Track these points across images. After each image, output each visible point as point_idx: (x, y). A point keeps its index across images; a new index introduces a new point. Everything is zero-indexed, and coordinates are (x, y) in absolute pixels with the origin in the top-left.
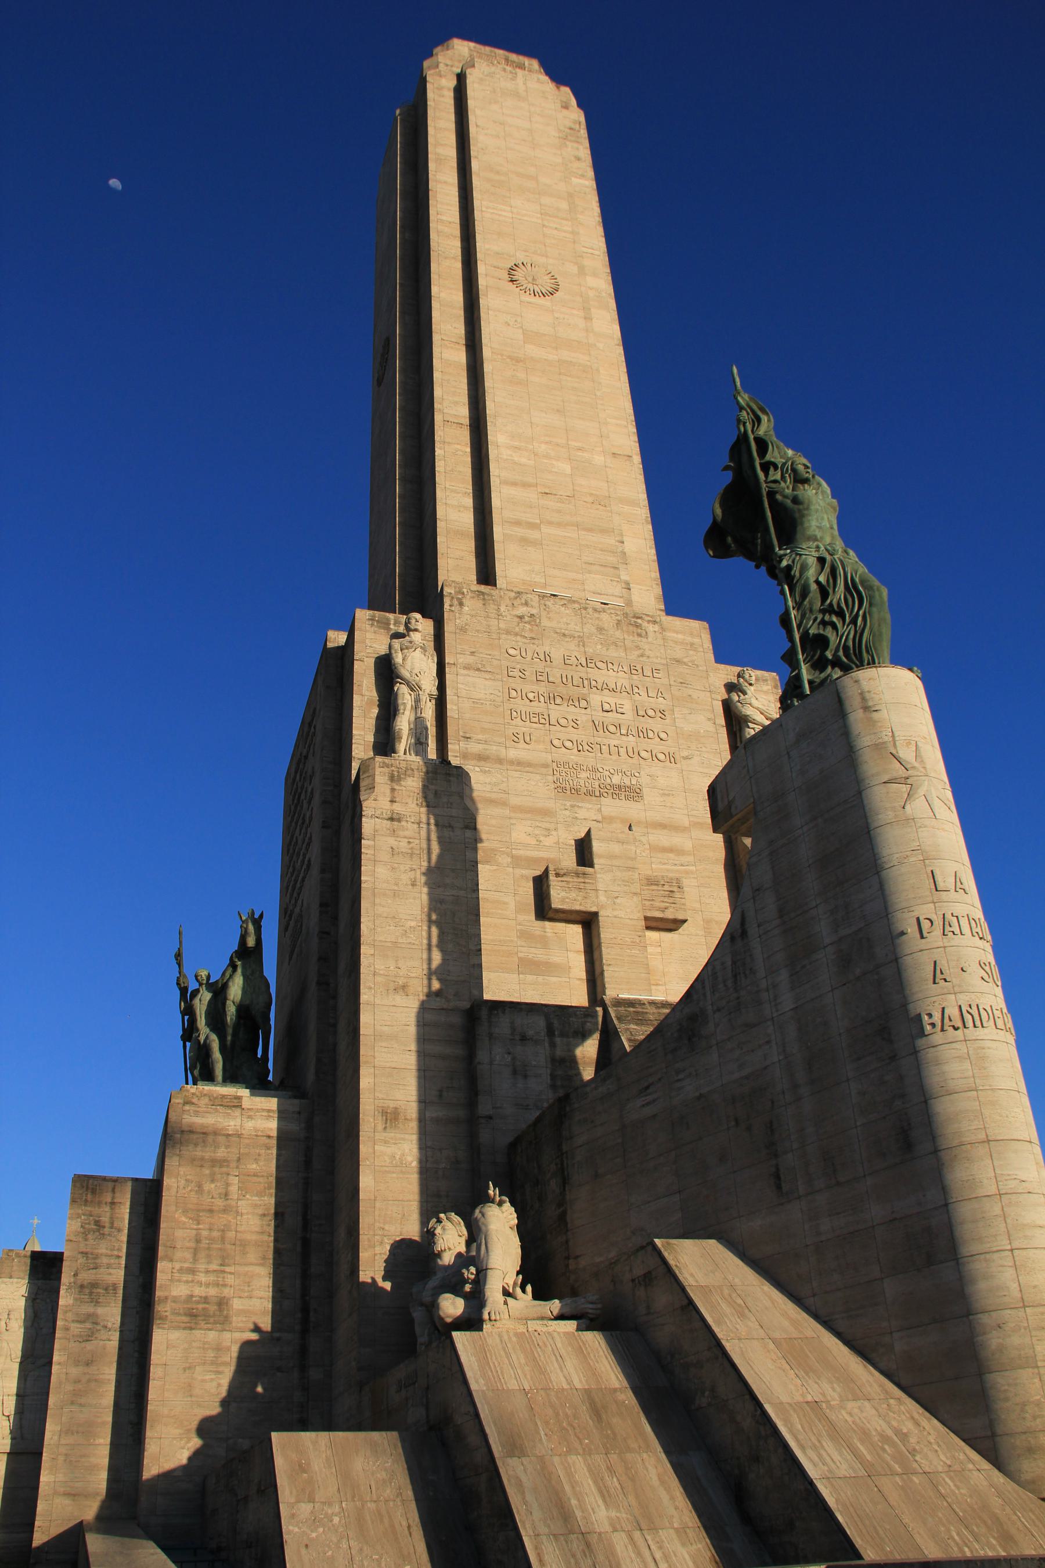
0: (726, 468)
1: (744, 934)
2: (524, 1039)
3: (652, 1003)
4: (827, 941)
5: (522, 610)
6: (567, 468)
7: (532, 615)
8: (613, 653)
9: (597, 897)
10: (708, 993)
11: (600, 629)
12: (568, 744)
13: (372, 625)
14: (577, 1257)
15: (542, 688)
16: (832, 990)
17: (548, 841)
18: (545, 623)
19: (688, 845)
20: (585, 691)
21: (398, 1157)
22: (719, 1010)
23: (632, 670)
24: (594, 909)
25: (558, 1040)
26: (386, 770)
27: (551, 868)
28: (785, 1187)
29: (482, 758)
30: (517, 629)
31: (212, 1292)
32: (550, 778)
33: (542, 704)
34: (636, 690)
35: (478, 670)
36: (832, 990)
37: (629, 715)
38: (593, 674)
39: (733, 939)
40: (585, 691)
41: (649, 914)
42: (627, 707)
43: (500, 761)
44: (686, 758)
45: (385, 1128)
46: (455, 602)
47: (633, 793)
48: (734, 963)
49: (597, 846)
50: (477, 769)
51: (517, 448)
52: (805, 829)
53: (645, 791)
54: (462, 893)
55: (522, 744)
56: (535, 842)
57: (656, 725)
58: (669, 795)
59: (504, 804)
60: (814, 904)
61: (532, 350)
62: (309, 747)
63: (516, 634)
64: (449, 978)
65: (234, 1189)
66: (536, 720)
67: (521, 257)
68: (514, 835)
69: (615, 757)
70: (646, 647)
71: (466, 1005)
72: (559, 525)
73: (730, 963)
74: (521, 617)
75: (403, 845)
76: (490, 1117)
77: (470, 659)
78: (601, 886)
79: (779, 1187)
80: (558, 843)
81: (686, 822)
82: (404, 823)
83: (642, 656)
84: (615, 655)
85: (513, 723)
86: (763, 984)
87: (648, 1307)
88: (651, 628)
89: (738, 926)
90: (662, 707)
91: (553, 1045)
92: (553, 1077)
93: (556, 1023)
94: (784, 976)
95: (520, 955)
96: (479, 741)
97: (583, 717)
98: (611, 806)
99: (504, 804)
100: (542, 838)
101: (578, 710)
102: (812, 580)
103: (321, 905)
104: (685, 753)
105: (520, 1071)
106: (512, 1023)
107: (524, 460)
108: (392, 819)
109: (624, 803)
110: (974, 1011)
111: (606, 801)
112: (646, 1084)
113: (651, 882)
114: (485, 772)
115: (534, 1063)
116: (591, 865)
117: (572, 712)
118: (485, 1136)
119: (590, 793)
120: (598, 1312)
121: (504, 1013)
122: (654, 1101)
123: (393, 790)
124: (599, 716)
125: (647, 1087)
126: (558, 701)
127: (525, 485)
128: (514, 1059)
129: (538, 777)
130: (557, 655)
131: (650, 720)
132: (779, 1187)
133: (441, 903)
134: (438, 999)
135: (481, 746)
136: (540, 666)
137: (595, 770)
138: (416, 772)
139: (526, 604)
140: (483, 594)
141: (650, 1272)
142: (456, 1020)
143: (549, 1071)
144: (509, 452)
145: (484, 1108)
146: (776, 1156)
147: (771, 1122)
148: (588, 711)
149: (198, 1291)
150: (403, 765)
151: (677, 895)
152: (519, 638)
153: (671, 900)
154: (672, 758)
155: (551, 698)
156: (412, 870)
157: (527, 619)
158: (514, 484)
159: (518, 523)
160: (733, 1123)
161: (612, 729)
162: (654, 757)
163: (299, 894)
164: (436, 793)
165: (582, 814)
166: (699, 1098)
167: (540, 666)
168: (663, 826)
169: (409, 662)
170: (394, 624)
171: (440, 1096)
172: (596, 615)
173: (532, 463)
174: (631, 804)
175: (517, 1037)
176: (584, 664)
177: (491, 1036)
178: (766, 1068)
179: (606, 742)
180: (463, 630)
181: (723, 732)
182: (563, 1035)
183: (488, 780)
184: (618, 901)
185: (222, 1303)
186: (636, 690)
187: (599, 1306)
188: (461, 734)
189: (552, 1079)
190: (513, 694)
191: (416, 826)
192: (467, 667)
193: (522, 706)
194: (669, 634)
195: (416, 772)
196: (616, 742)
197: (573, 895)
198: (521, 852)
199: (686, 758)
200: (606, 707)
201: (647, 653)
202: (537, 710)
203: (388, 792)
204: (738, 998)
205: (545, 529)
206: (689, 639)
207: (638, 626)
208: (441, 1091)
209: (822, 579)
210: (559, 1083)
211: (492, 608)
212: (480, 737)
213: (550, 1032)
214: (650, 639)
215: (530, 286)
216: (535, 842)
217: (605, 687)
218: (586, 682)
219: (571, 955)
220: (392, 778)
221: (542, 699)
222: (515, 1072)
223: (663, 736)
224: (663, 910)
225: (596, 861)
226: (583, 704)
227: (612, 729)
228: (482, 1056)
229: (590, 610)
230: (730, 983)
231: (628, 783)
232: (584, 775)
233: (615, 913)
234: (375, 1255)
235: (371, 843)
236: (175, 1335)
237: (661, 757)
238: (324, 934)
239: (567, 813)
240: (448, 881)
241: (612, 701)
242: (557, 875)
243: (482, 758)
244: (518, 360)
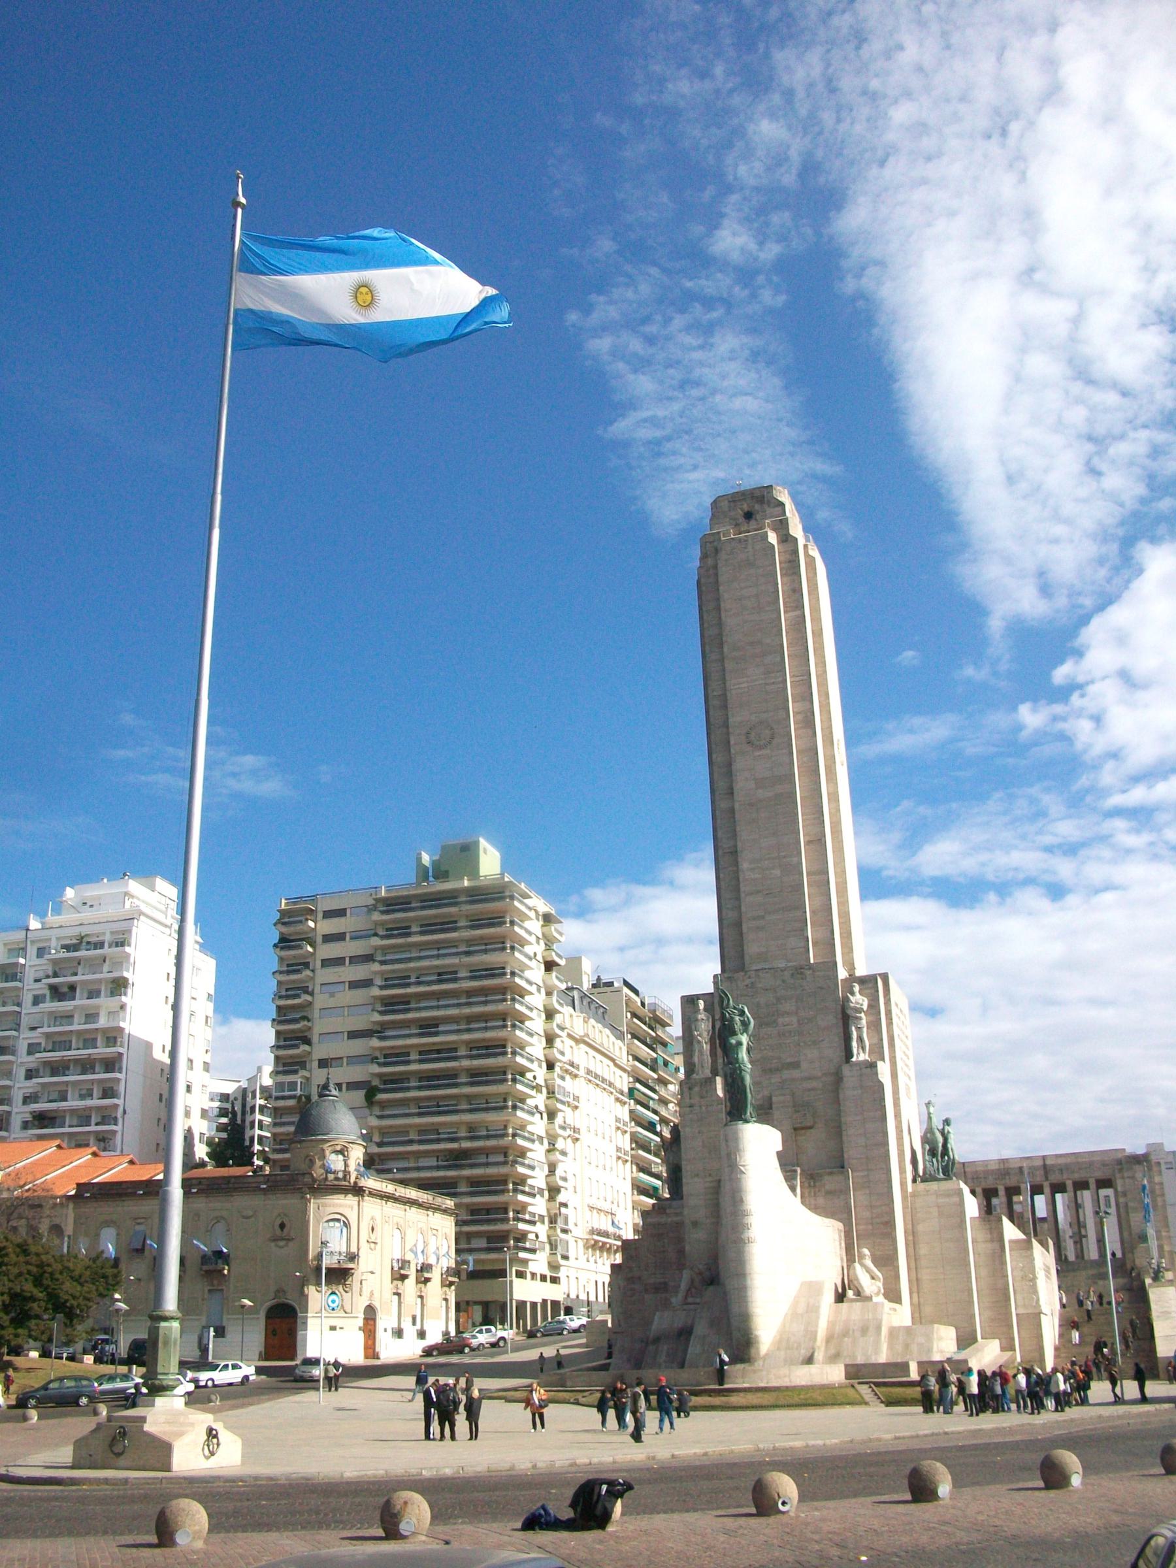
6: (777, 872)
47: (796, 1065)
61: (761, 794)
88: (808, 972)
98: (786, 1074)
107: (757, 876)
127: (758, 892)
154: (815, 1043)
158: (751, 894)
168: (810, 1078)
185: (665, 1284)
244: (751, 805)
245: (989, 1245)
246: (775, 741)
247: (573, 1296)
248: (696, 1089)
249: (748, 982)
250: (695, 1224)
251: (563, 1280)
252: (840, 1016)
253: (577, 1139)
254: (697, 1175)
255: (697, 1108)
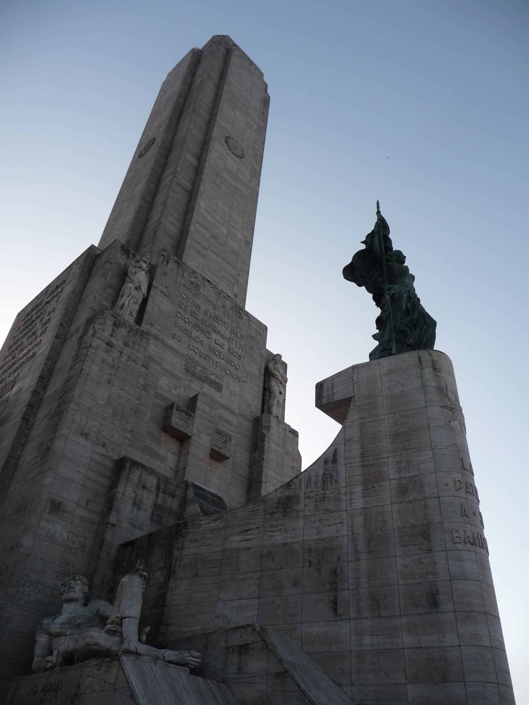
0: (363, 242)
1: (334, 461)
2: (144, 487)
3: (210, 492)
4: (392, 477)
5: (193, 280)
6: (225, 232)
7: (197, 285)
8: (226, 319)
9: (193, 429)
10: (303, 487)
11: (224, 306)
12: (196, 350)
13: (122, 250)
14: (168, 625)
15: (192, 319)
16: (392, 504)
17: (174, 392)
18: (202, 291)
19: (236, 423)
20: (210, 330)
21: (52, 532)
22: (309, 498)
23: (232, 331)
24: (189, 434)
25: (161, 494)
26: (113, 319)
27: (175, 405)
28: (340, 611)
29: (156, 337)
30: (189, 287)
32: (184, 362)
33: (190, 327)
34: (231, 341)
35: (166, 296)
36: (392, 504)
37: (225, 351)
38: (215, 324)
39: (326, 462)
40: (210, 330)
41: (213, 448)
42: (226, 346)
43: (163, 343)
44: (244, 382)
45: (50, 512)
46: (165, 260)
47: (219, 388)
48: (324, 474)
49: (199, 404)
50: (152, 342)
51: (207, 211)
52: (386, 417)
53: (224, 388)
54: (131, 398)
55: (176, 341)
56: (168, 390)
57: (236, 361)
58: (233, 395)
59: (159, 364)
60: (386, 456)
61: (226, 175)
62: (54, 296)
63: (188, 289)
64: (112, 439)
66: (185, 332)
67: (232, 135)
68: (159, 381)
69: (214, 367)
70: (241, 324)
71: (116, 457)
72: (215, 254)
73: (321, 474)
74: (192, 283)
75: (110, 360)
76: (114, 525)
77: (165, 290)
78: (196, 424)
79: (335, 610)
80: (178, 395)
81: (237, 411)
82: (114, 349)
83: (238, 327)
84: (227, 321)
85: (175, 328)
86: (344, 490)
87: (240, 669)
89: (331, 456)
90: (240, 354)
91: (157, 496)
92: (153, 514)
93: (162, 485)
94: (359, 489)
95: (146, 443)
96: (157, 329)
97: (206, 342)
98: (207, 389)
99: (159, 364)
100: (172, 389)
101: (205, 337)
102: (404, 305)
103: (40, 376)
104: (245, 380)
105: (137, 504)
106: (140, 476)
107: (208, 218)
108: (108, 344)
109: (212, 389)
110: (479, 537)
111: (205, 385)
112: (247, 528)
113: (219, 432)
114: (155, 345)
115: (145, 502)
116: (194, 412)
117: (202, 337)
118: (108, 536)
119: (199, 378)
120: (198, 664)
121: (138, 469)
122: (250, 539)
123: (113, 330)
124: (213, 344)
125: (248, 530)
126: (197, 328)
127: (206, 229)
128: (136, 496)
129: (178, 359)
130: (203, 307)
131: (234, 357)
132: (335, 610)
133: (119, 398)
134: (103, 449)
135: (157, 332)
136: (194, 309)
137: (204, 368)
138: (127, 327)
139: (196, 278)
140: (179, 263)
141: (247, 645)
142: (109, 464)
143: (151, 510)
144: (204, 211)
145: (113, 518)
146: (336, 590)
147: (336, 569)
148: (209, 340)
150: (122, 321)
151: (228, 444)
152: (188, 291)
153: (225, 445)
154: (239, 380)
155: (195, 326)
156: (110, 374)
157: (194, 285)
158: (202, 226)
159: (198, 243)
160: (307, 565)
161: (217, 353)
162: (231, 375)
163: (15, 371)
164: (134, 342)
165: (193, 386)
166: (284, 545)
167: (194, 309)
169: (138, 275)
170: (132, 255)
171: (87, 504)
172: (224, 299)
173: (212, 221)
174: (215, 392)
175: (141, 485)
176: (213, 317)
177: (128, 478)
178: (337, 537)
179: (213, 358)
180: (165, 274)
181: (262, 378)
182: (164, 492)
183: (155, 350)
184: (202, 435)
186: (231, 341)
187: (200, 660)
188: (150, 321)
189: (152, 515)
190: (179, 315)
191: (119, 353)
192: (162, 292)
193: (180, 322)
194: (251, 323)
195: (127, 327)
196: (217, 360)
197: (182, 423)
198: (161, 392)
199: (244, 382)
200: (217, 342)
201: (241, 327)
202: (187, 328)
203: (110, 330)
204: (324, 494)
205: (208, 251)
206: (259, 330)
207: (240, 313)
208: (88, 501)
209: (408, 306)
210: (155, 518)
212: (158, 327)
213: (158, 488)
214: (243, 322)
215: (233, 149)
216: (168, 390)
217: (219, 333)
218: (212, 326)
219: (170, 454)
220: (115, 324)
221: (190, 324)
222: (134, 504)
223: (237, 367)
224: (220, 448)
225: (197, 411)
226: (208, 335)
227: (217, 353)
228: (120, 488)
229: (222, 296)
230: (319, 485)
231: (217, 381)
232: (199, 368)
233: (199, 441)
234: (17, 592)
235: (94, 351)
237: (234, 376)
238: (35, 392)
239: (187, 382)
240: (127, 388)
241: (221, 340)
242: (177, 410)
243: (156, 337)
246: (242, 159)
248: (123, 331)
250: (56, 507)
254: (86, 435)
255: (115, 354)
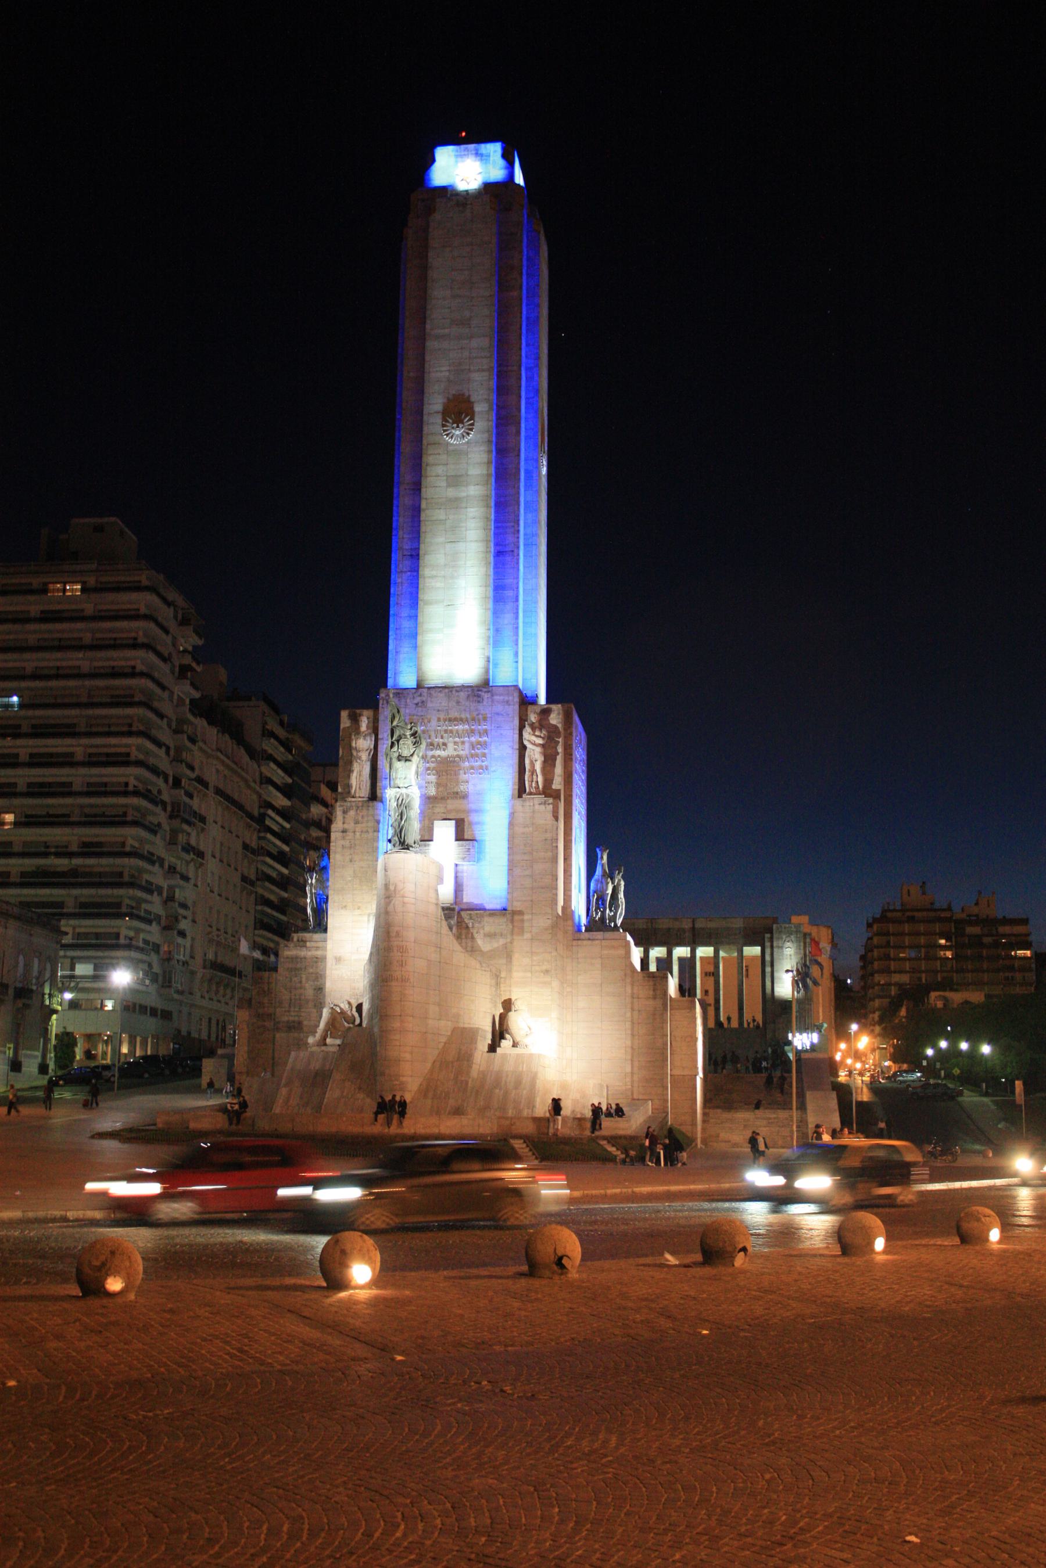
31: (296, 1019)
65: (304, 980)
74: (417, 704)
149: (291, 1019)
185: (300, 1023)
207: (479, 696)
211: (403, 701)
236: (283, 1035)
245: (651, 1002)
247: (184, 1033)
248: (352, 813)
249: (418, 700)
251: (175, 1016)
252: (517, 746)
253: (201, 865)
255: (350, 835)
